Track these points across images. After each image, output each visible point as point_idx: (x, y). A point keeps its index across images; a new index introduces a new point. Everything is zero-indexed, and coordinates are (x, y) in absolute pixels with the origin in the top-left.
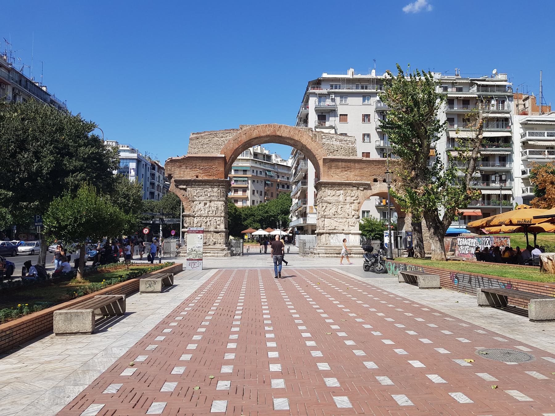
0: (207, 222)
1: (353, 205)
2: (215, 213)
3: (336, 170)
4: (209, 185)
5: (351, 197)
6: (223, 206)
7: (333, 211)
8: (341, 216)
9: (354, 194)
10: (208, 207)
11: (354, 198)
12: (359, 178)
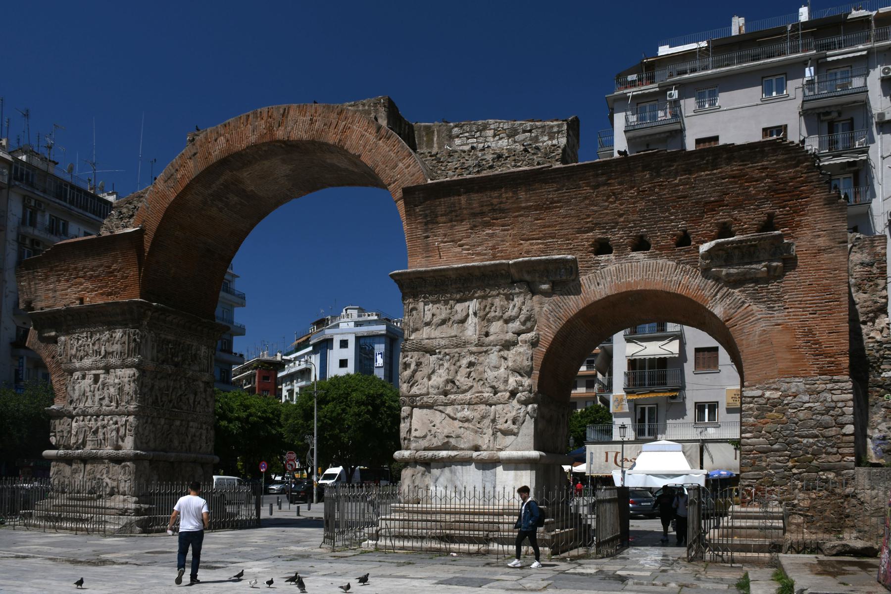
1: (511, 354)
3: (452, 227)
5: (507, 322)
7: (438, 380)
8: (468, 395)
9: (516, 309)
11: (516, 325)
12: (537, 246)
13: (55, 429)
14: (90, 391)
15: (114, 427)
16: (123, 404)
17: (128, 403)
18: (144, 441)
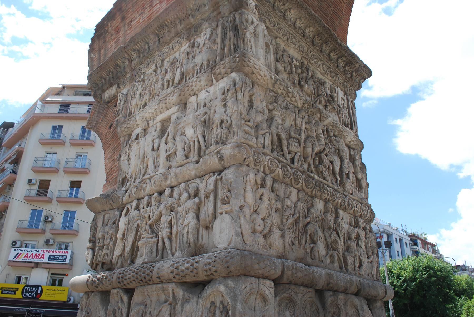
16: (212, 148)
18: (259, 229)
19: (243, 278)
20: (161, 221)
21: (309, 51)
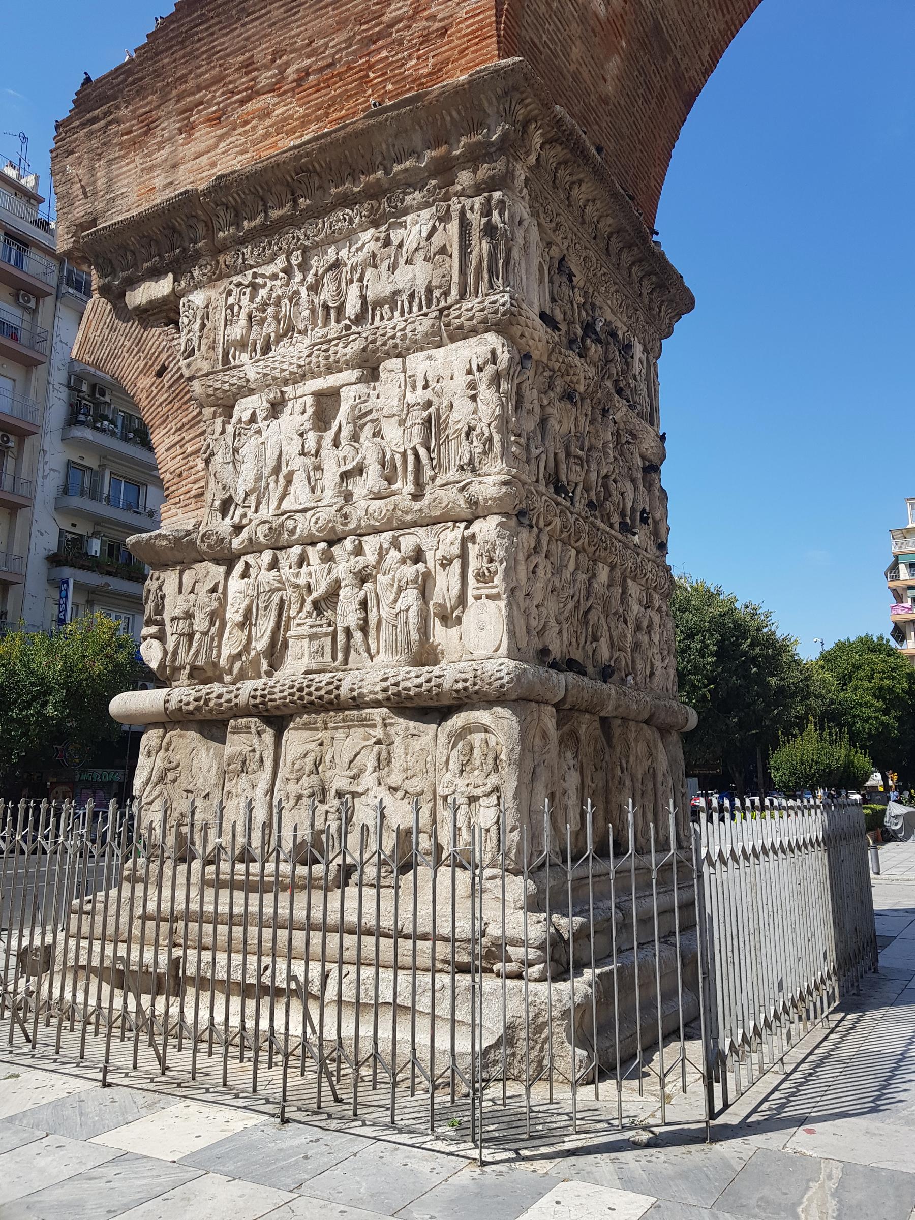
0: (332, 596)
2: (410, 488)
4: (347, 201)
6: (496, 379)
10: (346, 433)
13: (159, 610)
14: (303, 453)
15: (410, 571)
16: (452, 474)
17: (471, 466)
19: (521, 703)
20: (340, 598)
21: (599, 266)
